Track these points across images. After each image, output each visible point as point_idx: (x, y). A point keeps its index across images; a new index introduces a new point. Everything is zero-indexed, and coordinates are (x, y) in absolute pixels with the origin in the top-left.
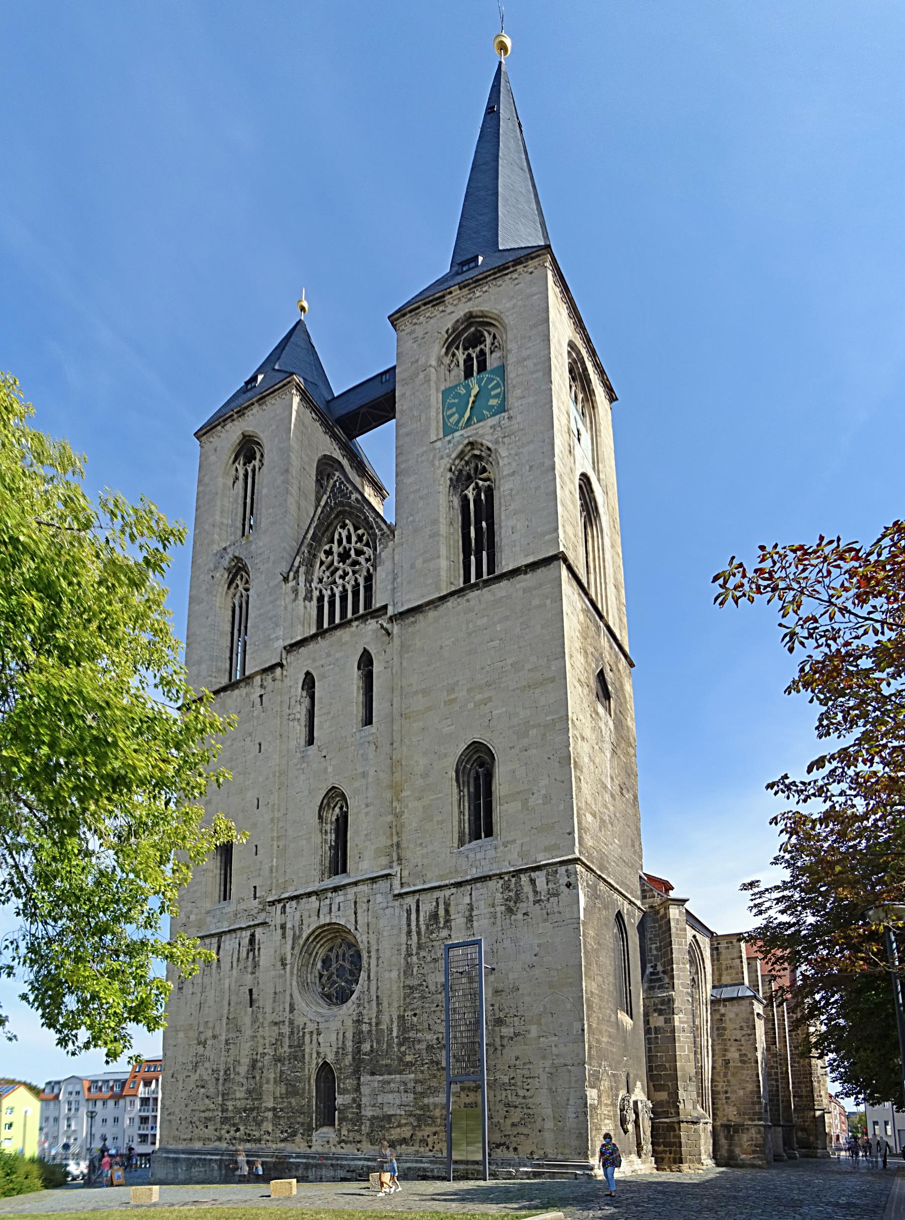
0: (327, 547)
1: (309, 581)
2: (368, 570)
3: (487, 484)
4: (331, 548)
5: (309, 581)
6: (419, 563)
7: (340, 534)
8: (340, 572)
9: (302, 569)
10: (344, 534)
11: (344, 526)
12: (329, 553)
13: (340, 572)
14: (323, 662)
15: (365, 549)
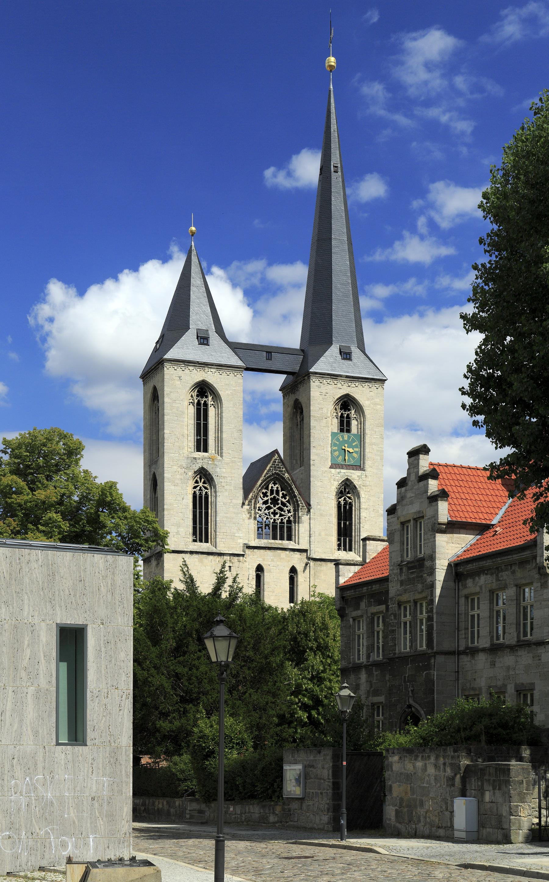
0: (264, 491)
1: (255, 508)
2: (289, 518)
3: (350, 501)
4: (266, 492)
5: (255, 508)
6: (323, 533)
7: (272, 487)
8: (272, 510)
9: (253, 501)
10: (275, 489)
11: (275, 484)
12: (265, 495)
13: (272, 510)
14: (269, 563)
15: (288, 504)
